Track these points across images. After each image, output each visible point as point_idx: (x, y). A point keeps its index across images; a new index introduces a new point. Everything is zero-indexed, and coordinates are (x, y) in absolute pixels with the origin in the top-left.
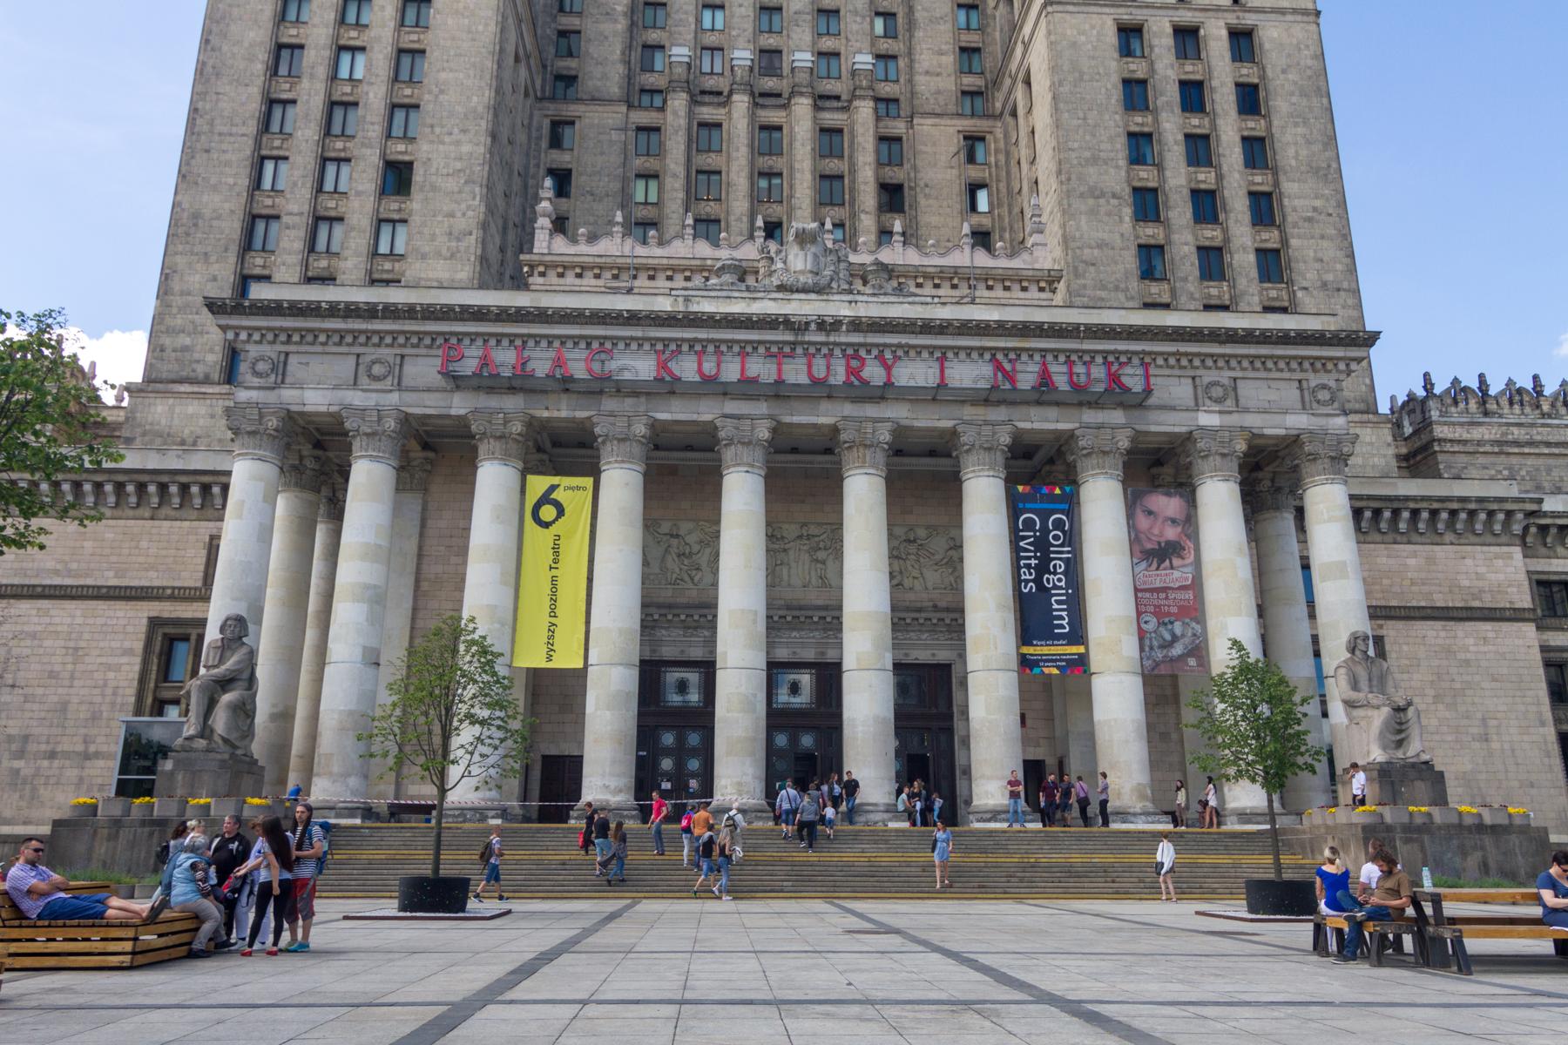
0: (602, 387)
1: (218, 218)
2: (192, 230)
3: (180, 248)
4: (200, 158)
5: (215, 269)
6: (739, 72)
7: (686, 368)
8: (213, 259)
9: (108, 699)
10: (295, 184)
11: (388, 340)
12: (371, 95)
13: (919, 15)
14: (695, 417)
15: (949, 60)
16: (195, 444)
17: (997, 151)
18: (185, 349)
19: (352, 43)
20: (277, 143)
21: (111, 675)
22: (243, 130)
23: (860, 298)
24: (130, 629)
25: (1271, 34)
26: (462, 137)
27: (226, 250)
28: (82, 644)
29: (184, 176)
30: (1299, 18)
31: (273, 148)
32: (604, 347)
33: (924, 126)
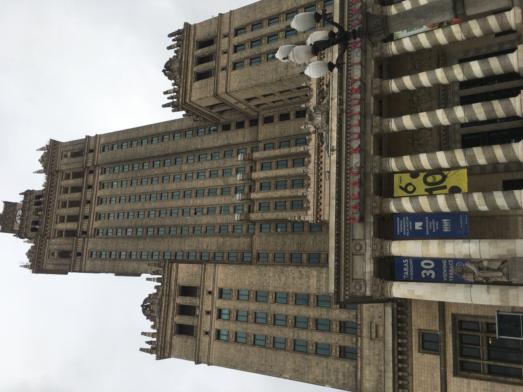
1: (295, 362)
3: (306, 376)
5: (314, 363)
7: (355, 144)
8: (310, 364)
10: (283, 334)
11: (348, 243)
12: (253, 308)
14: (372, 142)
15: (240, 131)
16: (381, 371)
18: (344, 375)
19: (235, 316)
20: (269, 342)
23: (331, 97)
25: (237, 24)
27: (307, 359)
29: (280, 375)
30: (232, 16)
31: (270, 343)
32: (349, 169)
33: (261, 137)
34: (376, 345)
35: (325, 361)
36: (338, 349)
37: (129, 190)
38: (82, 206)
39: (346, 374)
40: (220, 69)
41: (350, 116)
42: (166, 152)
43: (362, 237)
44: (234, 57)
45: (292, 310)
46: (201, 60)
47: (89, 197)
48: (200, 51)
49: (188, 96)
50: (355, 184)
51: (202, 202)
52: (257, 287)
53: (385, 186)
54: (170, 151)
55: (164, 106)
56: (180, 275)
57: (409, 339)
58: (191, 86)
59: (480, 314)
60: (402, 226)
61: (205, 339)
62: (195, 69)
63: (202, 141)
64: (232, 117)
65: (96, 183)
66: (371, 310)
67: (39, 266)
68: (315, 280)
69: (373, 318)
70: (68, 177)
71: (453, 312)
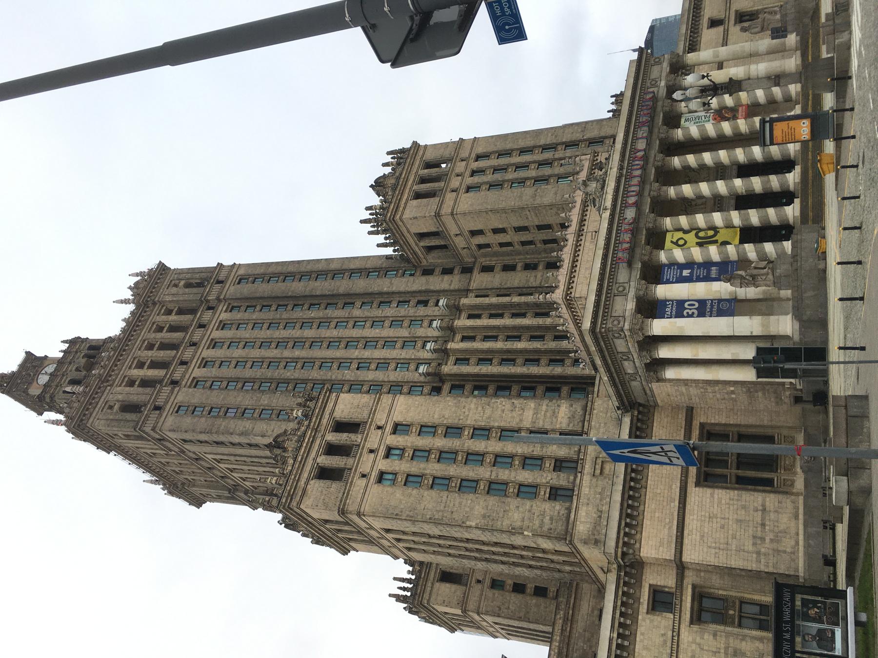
0: (636, 220)
1: (487, 507)
3: (499, 523)
4: (455, 516)
7: (632, 200)
8: (507, 508)
18: (551, 519)
20: (453, 485)
21: (723, 502)
22: (445, 497)
24: (701, 495)
25: (480, 150)
28: (707, 514)
33: (474, 285)
34: (600, 482)
35: (528, 503)
36: (548, 490)
37: (264, 334)
40: (449, 189)
41: (629, 177)
43: (627, 280)
44: (469, 181)
45: (494, 446)
46: (423, 181)
47: (196, 338)
48: (426, 171)
49: (400, 213)
50: (626, 231)
52: (450, 421)
53: (657, 239)
54: (341, 291)
55: (362, 222)
56: (340, 407)
58: (406, 204)
60: (668, 274)
61: (361, 483)
62: (415, 187)
65: (214, 322)
67: (82, 420)
68: (531, 412)
70: (169, 312)
71: (702, 421)
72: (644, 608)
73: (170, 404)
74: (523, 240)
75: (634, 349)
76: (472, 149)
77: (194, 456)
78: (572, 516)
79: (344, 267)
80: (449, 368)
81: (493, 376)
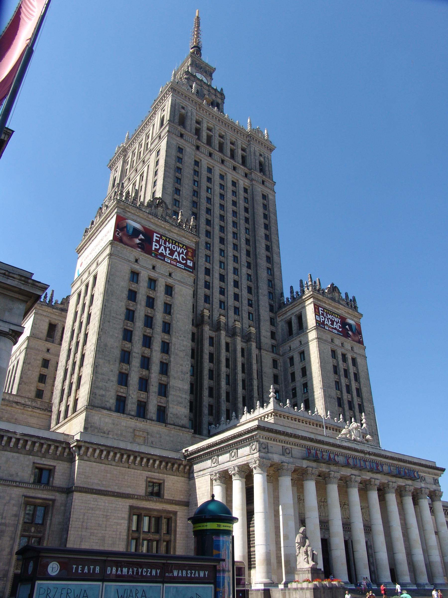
2: (104, 351)
6: (222, 324)
8: (111, 363)
9: (118, 536)
10: (136, 342)
12: (158, 316)
13: (261, 318)
15: (269, 334)
17: (281, 366)
18: (103, 396)
21: (119, 527)
24: (123, 509)
25: (359, 360)
26: (184, 338)
27: (115, 361)
28: (109, 514)
35: (115, 379)
36: (124, 395)
38: (220, 154)
39: (104, 398)
42: (258, 256)
44: (339, 353)
51: (216, 278)
52: (174, 325)
54: (259, 260)
57: (157, 471)
59: (177, 536)
63: (265, 295)
64: (280, 331)
66: (158, 436)
68: (181, 386)
69: (152, 436)
70: (243, 150)
71: (178, 513)
72: (38, 460)
73: (185, 143)
74: (297, 389)
75: (241, 461)
76: (359, 354)
77: (146, 159)
78: (105, 412)
79: (275, 263)
80: (207, 331)
81: (202, 363)
